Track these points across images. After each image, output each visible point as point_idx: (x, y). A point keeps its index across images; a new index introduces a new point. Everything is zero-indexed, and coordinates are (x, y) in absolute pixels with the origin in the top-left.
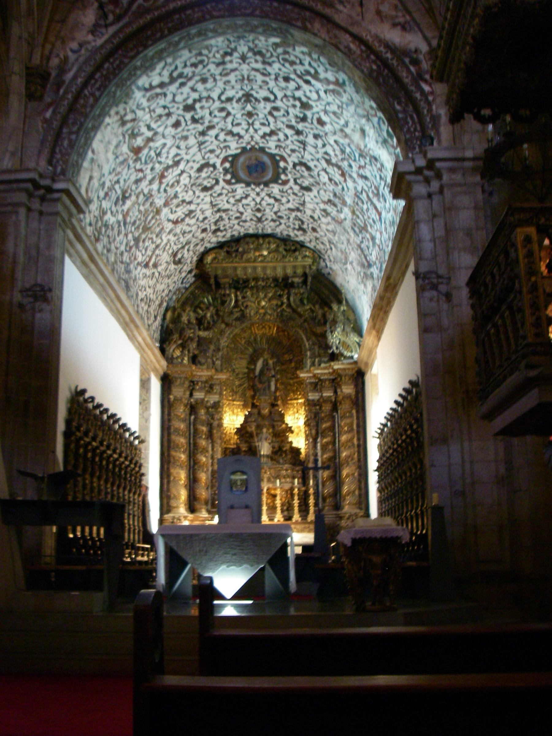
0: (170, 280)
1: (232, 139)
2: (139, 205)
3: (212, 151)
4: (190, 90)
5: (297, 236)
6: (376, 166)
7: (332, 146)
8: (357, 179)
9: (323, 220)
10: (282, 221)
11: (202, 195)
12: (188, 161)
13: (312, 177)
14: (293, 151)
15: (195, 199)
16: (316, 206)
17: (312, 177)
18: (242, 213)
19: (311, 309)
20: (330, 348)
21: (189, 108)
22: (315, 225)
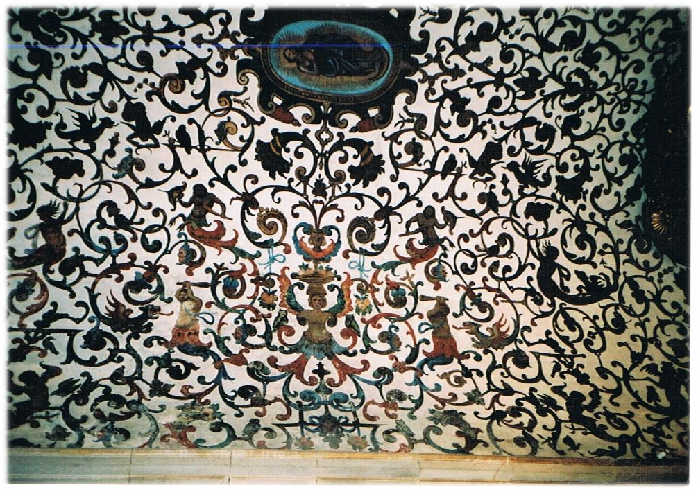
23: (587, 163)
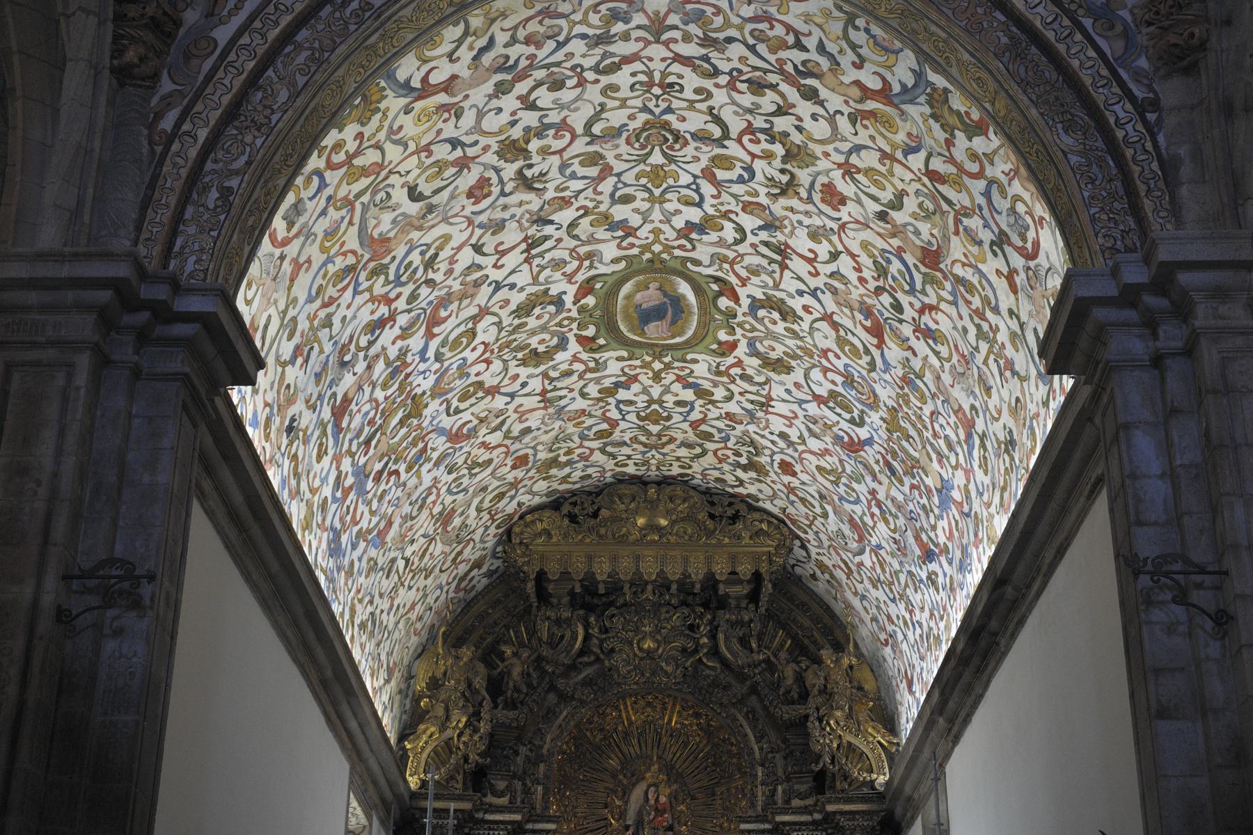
0: (430, 580)
1: (608, 235)
2: (374, 385)
3: (558, 264)
4: (518, 104)
5: (741, 483)
6: (968, 303)
7: (853, 256)
8: (913, 342)
9: (814, 444)
10: (710, 446)
11: (524, 372)
12: (498, 286)
13: (795, 335)
14: (755, 271)
15: (506, 381)
16: (795, 407)
17: (795, 335)
18: (614, 424)
19: (767, 661)
20: (819, 757)
21: (512, 149)
22: (790, 455)
23: (763, 131)
